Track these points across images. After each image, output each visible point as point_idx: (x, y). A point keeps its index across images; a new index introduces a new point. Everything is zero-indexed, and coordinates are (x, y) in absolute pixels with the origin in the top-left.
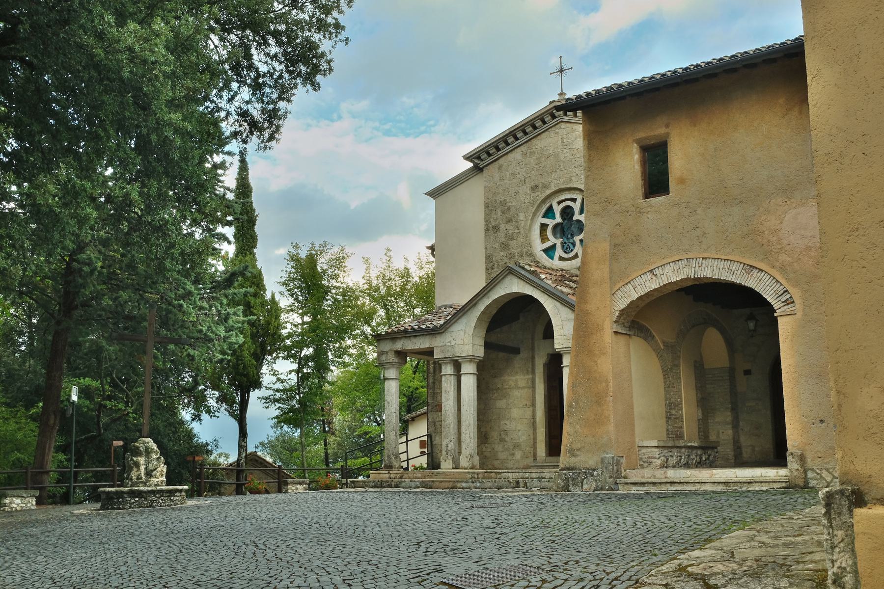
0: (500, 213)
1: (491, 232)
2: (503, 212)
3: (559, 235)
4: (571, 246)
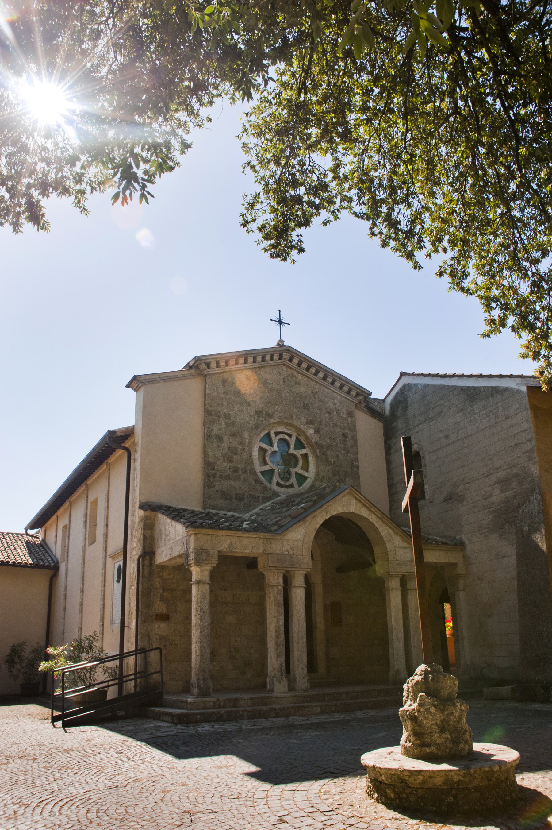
2: (227, 425)
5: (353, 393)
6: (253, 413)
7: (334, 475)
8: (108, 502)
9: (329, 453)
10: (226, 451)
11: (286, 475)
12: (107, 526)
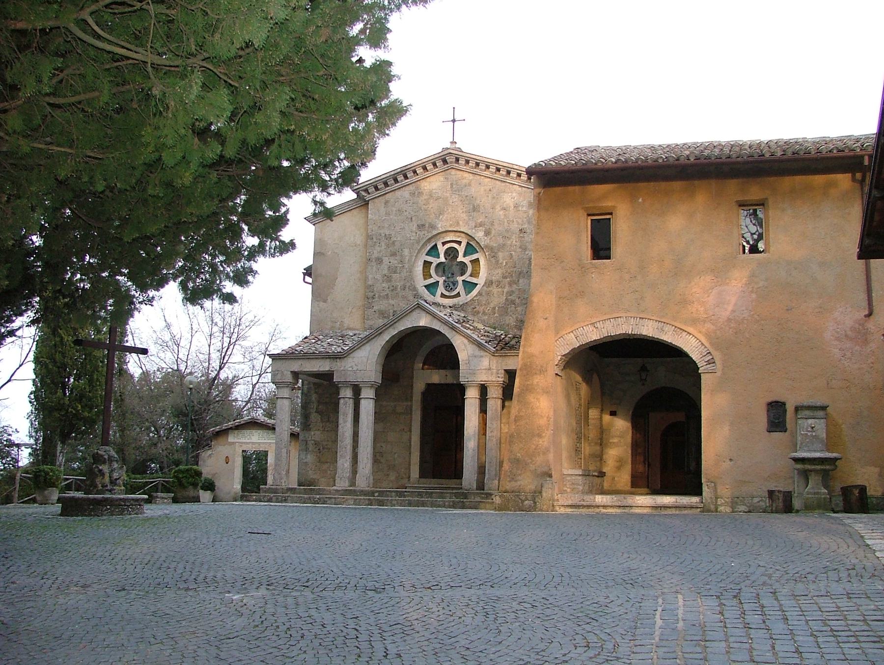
1: (374, 264)
2: (388, 246)
3: (440, 274)
4: (451, 285)
7: (505, 277)
9: (500, 255)
10: (386, 272)
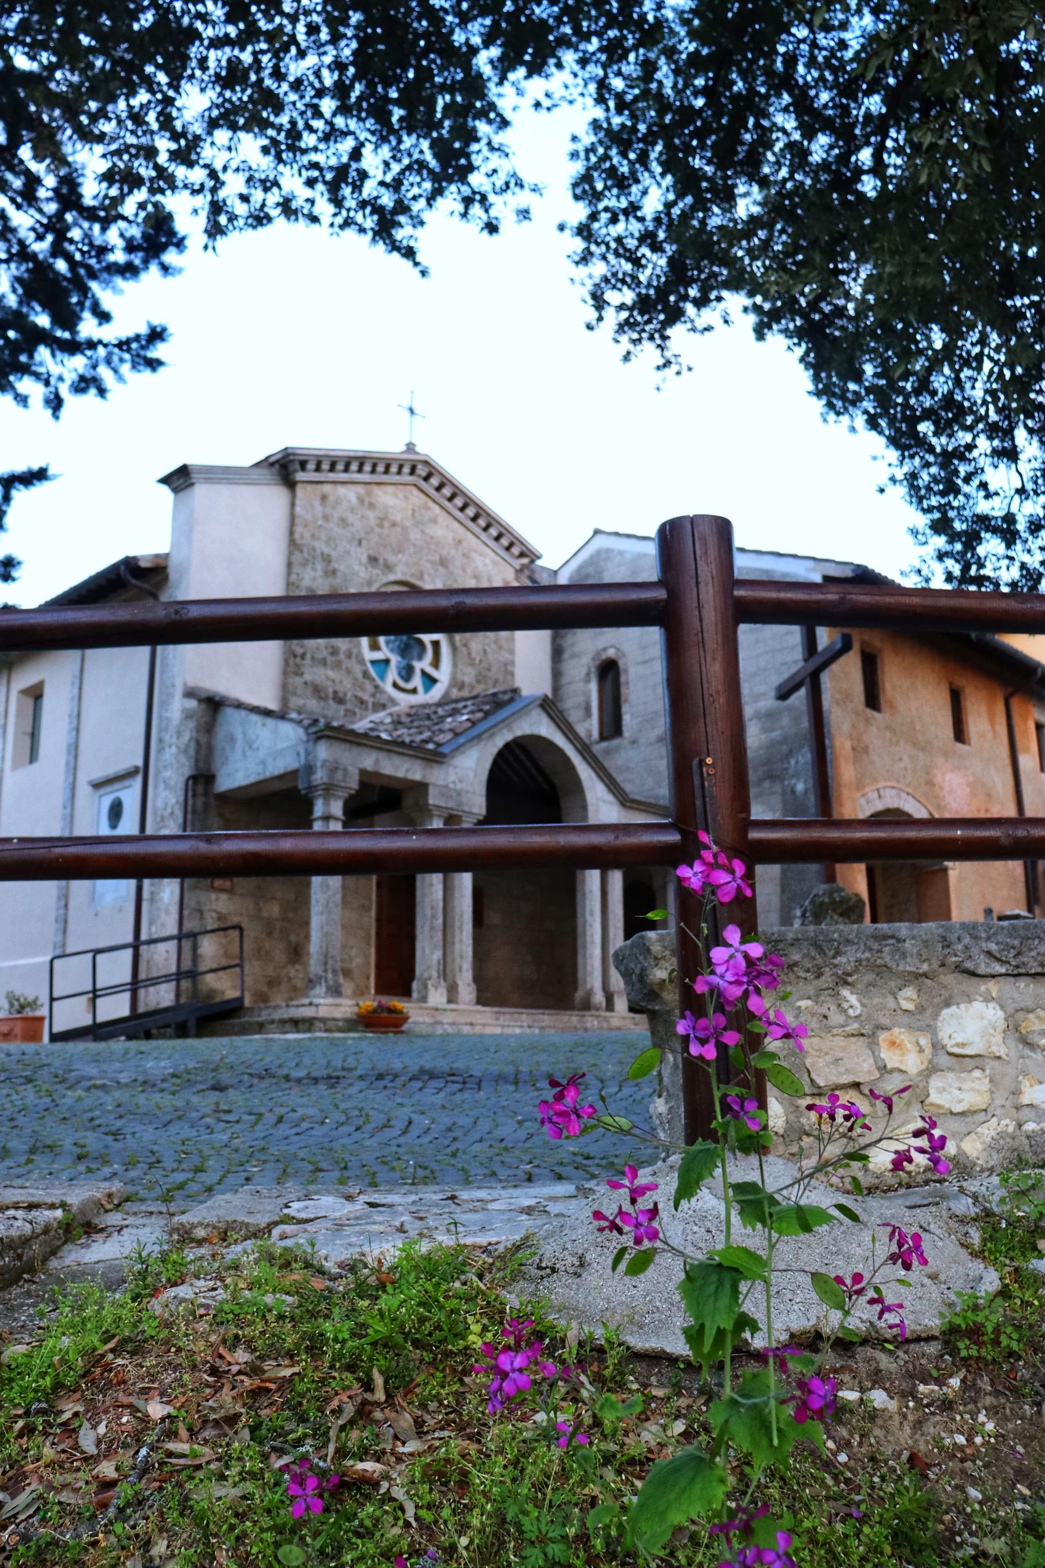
0: (319, 573)
5: (516, 551)
6: (364, 559)
7: (478, 681)
8: (80, 688)
11: (407, 673)
12: (78, 730)
